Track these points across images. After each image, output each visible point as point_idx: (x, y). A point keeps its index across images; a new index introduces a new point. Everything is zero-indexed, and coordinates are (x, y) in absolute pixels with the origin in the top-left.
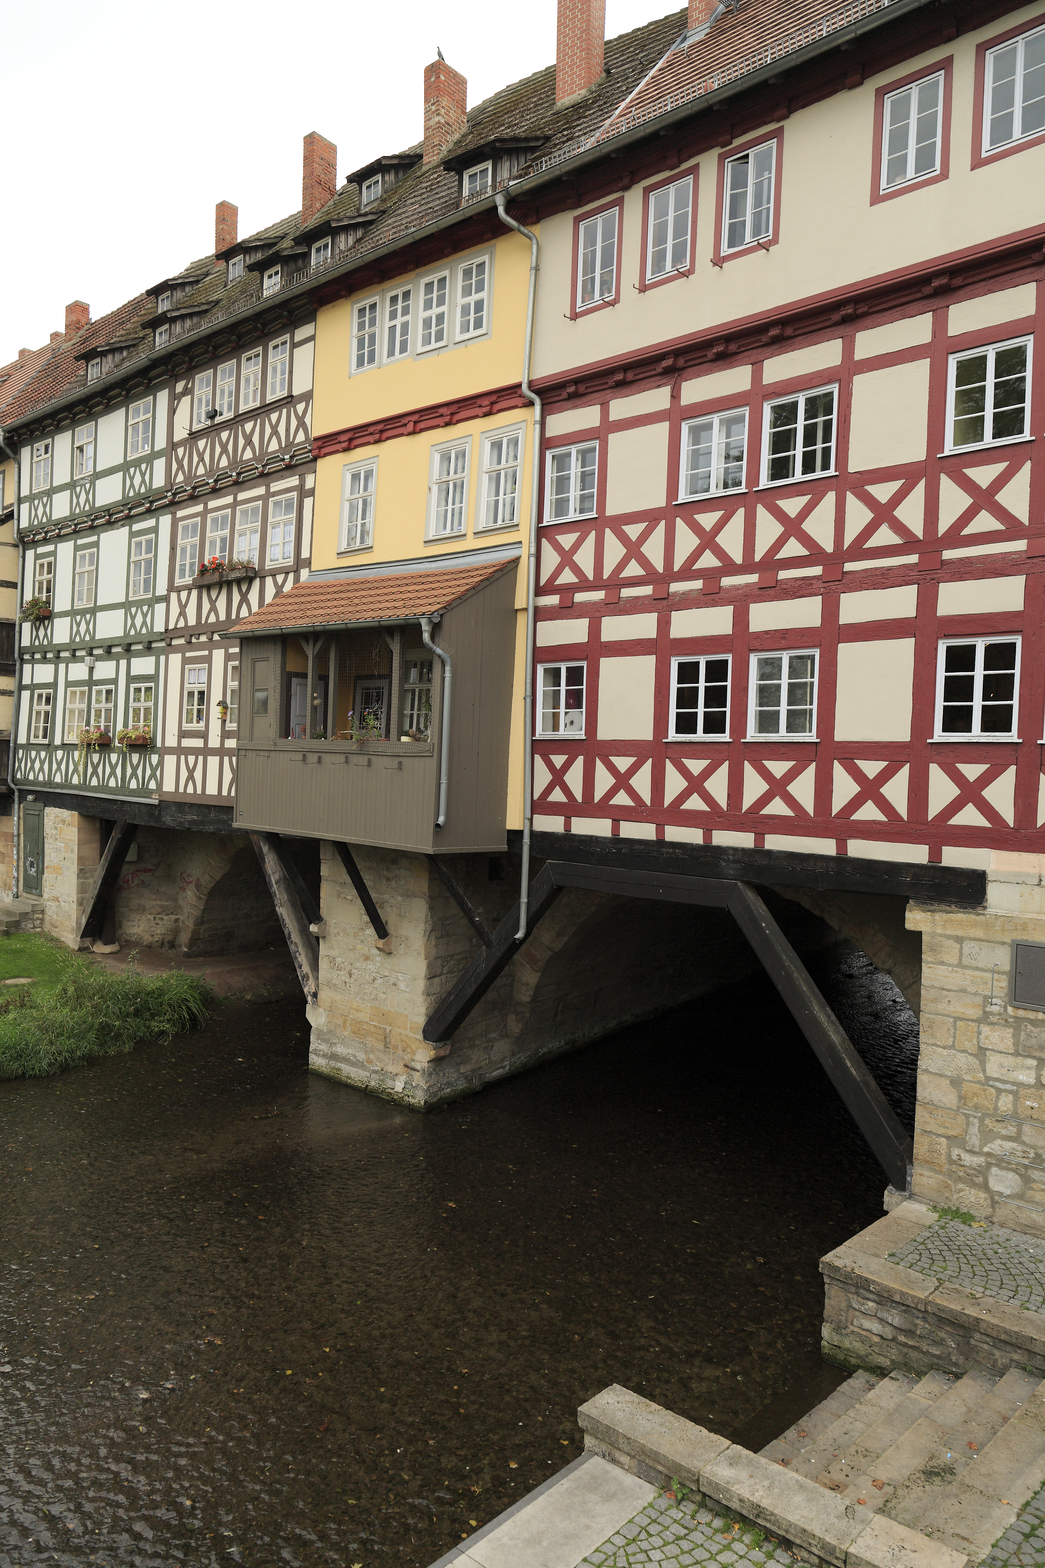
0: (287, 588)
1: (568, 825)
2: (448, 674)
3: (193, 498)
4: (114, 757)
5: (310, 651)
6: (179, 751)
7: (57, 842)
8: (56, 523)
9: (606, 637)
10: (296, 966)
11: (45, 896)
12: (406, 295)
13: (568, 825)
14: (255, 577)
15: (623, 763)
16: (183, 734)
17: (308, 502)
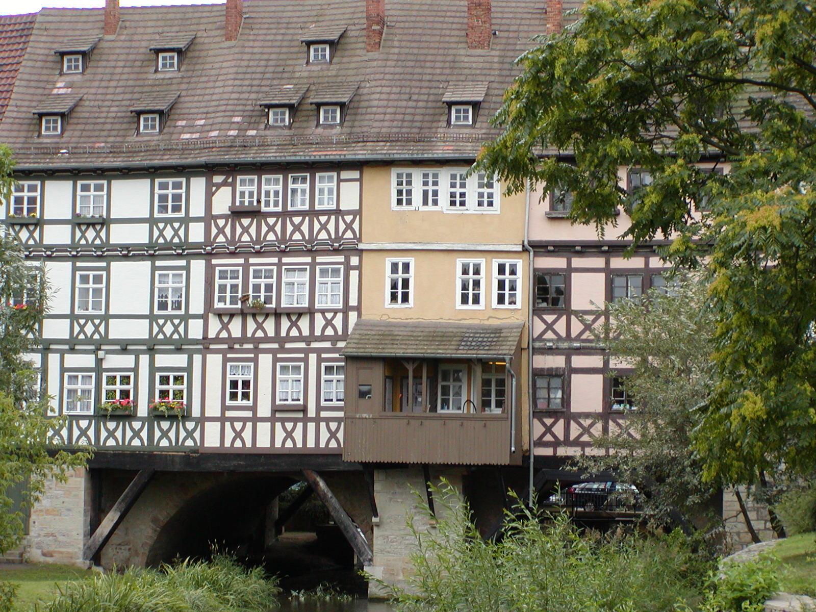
0: (338, 321)
1: (555, 451)
2: (514, 383)
3: (233, 254)
4: (137, 425)
5: (410, 368)
6: (222, 419)
7: (51, 491)
8: (49, 248)
9: (574, 365)
10: (353, 546)
11: (32, 533)
12: (435, 176)
13: (555, 451)
14: (306, 313)
15: (587, 422)
16: (224, 408)
17: (354, 275)
